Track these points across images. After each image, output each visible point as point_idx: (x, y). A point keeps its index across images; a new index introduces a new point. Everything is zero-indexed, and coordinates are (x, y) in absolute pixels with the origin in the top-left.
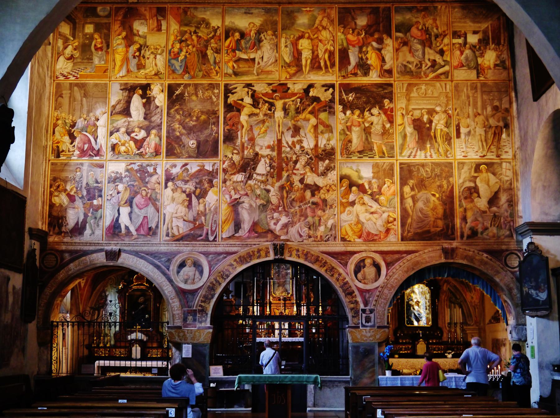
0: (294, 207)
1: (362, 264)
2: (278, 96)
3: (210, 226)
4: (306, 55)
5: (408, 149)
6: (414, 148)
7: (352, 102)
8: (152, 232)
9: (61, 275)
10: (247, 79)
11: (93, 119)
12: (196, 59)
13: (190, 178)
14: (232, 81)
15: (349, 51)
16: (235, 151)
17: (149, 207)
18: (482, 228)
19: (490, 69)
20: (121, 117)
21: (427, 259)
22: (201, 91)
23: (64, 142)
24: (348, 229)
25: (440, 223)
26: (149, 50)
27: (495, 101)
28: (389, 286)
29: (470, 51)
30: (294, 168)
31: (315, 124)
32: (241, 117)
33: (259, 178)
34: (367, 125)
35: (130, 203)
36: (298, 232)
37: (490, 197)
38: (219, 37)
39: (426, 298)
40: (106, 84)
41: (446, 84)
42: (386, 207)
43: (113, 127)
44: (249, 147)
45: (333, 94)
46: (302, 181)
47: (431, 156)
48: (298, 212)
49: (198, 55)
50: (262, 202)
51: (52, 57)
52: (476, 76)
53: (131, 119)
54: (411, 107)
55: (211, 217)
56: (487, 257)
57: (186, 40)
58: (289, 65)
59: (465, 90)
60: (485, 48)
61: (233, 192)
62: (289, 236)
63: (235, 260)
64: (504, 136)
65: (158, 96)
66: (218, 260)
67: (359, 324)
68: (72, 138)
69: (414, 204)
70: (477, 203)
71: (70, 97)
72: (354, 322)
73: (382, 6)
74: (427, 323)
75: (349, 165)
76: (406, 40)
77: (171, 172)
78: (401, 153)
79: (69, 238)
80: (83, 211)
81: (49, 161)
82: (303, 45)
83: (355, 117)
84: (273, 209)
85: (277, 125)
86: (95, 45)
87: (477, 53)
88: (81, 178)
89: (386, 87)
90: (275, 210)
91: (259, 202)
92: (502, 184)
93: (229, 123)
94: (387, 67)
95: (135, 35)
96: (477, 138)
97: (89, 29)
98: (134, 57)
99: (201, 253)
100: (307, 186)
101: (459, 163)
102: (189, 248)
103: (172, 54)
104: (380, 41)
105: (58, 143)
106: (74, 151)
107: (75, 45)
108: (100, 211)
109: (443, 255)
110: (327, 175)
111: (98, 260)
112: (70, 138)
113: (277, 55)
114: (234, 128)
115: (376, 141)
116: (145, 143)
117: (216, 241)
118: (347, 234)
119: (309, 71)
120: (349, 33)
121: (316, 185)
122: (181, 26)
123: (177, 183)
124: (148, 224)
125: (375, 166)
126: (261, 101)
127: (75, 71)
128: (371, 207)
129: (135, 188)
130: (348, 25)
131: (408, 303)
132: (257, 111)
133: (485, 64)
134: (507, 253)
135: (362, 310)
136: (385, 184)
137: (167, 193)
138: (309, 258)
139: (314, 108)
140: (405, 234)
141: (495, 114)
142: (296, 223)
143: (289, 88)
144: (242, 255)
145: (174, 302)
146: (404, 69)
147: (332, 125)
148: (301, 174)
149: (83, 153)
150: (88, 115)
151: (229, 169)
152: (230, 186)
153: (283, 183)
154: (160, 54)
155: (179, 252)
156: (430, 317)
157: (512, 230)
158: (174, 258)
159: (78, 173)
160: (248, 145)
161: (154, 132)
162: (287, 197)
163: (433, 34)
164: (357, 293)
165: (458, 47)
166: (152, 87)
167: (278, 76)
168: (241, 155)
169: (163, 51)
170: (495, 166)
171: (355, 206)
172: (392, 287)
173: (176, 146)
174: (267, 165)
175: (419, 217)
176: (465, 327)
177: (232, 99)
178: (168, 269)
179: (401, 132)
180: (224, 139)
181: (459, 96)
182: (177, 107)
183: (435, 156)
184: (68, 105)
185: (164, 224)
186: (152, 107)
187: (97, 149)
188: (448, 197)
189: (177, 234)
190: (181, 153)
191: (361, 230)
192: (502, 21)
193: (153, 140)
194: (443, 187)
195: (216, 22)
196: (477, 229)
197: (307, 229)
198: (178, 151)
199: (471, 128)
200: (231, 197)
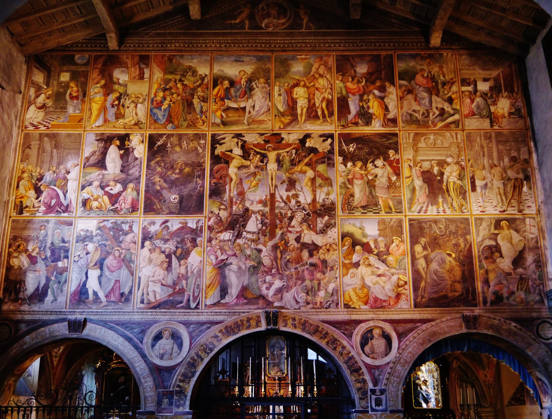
0: (290, 269)
1: (369, 335)
3: (192, 290)
4: (302, 104)
6: (424, 203)
7: (353, 152)
8: (125, 298)
9: (15, 350)
10: (236, 129)
11: (63, 171)
12: (181, 108)
13: (170, 236)
14: (220, 131)
15: (349, 99)
16: (223, 207)
17: (122, 269)
18: (508, 293)
19: (505, 117)
20: (95, 170)
21: (446, 330)
22: (185, 142)
23: (28, 197)
24: (352, 294)
25: (459, 287)
26: (129, 99)
27: (512, 152)
28: (402, 361)
29: (481, 99)
30: (289, 225)
31: (312, 177)
33: (250, 236)
34: (370, 178)
35: (100, 264)
36: (294, 297)
37: (515, 257)
38: (207, 85)
39: (433, 377)
40: (80, 134)
41: (456, 134)
42: (395, 268)
43: (86, 180)
44: (238, 202)
45: (332, 144)
46: (298, 239)
47: (444, 211)
48: (294, 275)
49: (183, 104)
50: (253, 263)
51: (22, 106)
52: (489, 126)
53: (106, 172)
54: (419, 158)
55: (194, 280)
56: (515, 327)
57: (171, 88)
58: (283, 115)
59: (478, 140)
60: (498, 96)
61: (219, 252)
62: (284, 303)
63: (221, 331)
64: (525, 189)
65: (137, 147)
66: (200, 331)
67: (367, 407)
68: (38, 192)
69: (428, 265)
70: (500, 263)
71: (39, 149)
72: (362, 405)
73: (383, 53)
74: (437, 405)
75: (352, 222)
76: (411, 88)
77: (149, 230)
78: (410, 208)
79: (27, 305)
80: (46, 274)
81: (10, 217)
82: (298, 93)
83: (357, 169)
84: (266, 272)
85: (270, 178)
86: (70, 94)
87: (489, 101)
88: (46, 236)
89: (390, 137)
90: (268, 272)
91: (249, 263)
92: (526, 242)
93: (216, 175)
94: (391, 116)
95: (115, 83)
96: (494, 191)
97: (65, 77)
98: (113, 106)
99: (180, 322)
100: (304, 246)
101: (476, 219)
102: (166, 317)
103: (154, 103)
104: (382, 89)
105: (22, 197)
106: (40, 207)
107: (48, 93)
108: (65, 274)
109: (463, 324)
110: (326, 233)
111: (59, 331)
112: (36, 193)
113: (270, 104)
114: (221, 181)
115: (382, 195)
116: (121, 198)
117: (199, 309)
118: (352, 300)
119: (305, 120)
120: (348, 81)
121: (314, 244)
122: (165, 74)
123: (155, 242)
124: (120, 289)
125: (382, 222)
126: (252, 153)
127: (46, 120)
128: (378, 268)
129: (107, 248)
130: (347, 73)
131: (414, 381)
133: (498, 112)
134: (539, 321)
135: (371, 390)
136: (393, 242)
137: (143, 254)
138: (307, 328)
139: (311, 159)
140: (419, 300)
141: (513, 165)
142: (291, 287)
143: (283, 139)
144: (229, 324)
145: (146, 382)
147: (332, 178)
148: (297, 232)
149: (50, 209)
150: (58, 168)
151: (215, 226)
152: (216, 246)
153: (276, 242)
154: (141, 103)
155: (156, 322)
156: (440, 398)
157: (543, 295)
158: (148, 328)
159: (42, 232)
160: (237, 199)
161: (131, 185)
162: (281, 257)
163: (439, 81)
164: (364, 369)
165: (468, 95)
166: (131, 137)
167: (271, 125)
169: (144, 100)
170: (518, 222)
171: (360, 268)
172: (406, 362)
173: (156, 201)
175: (434, 280)
176: (479, 410)
177: (219, 150)
178: (141, 342)
179: (409, 186)
180: (210, 194)
181: (472, 146)
182: (158, 159)
183: (448, 212)
184: (36, 156)
187: (65, 204)
188: (466, 257)
189: (153, 300)
190: (161, 208)
191: (367, 295)
192: (513, 69)
193: (130, 194)
194: (460, 246)
195: (203, 70)
196: (502, 294)
197: (304, 294)
198: (158, 206)
199: (488, 180)
200: (217, 258)
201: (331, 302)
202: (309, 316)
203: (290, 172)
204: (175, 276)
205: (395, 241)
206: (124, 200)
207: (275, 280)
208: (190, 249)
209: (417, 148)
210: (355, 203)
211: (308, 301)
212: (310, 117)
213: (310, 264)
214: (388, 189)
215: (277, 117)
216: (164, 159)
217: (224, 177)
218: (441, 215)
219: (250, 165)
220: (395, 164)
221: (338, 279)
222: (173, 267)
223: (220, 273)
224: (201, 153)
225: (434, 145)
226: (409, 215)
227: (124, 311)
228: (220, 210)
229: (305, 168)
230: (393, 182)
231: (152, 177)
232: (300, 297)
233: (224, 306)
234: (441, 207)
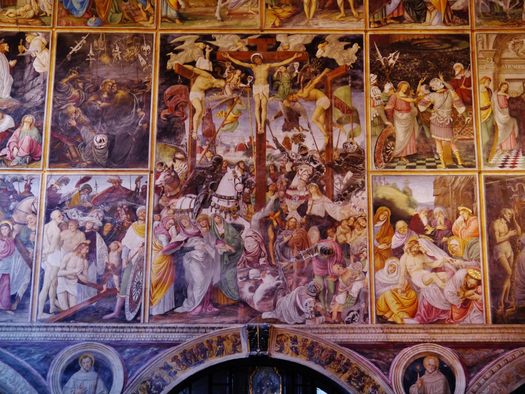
0: (289, 258)
1: (418, 367)
2: (260, 57)
3: (129, 290)
5: (500, 152)
6: (511, 151)
7: (395, 67)
13: (93, 203)
16: (179, 156)
17: (14, 256)
22: (117, 48)
24: (390, 299)
30: (288, 187)
31: (326, 107)
32: (191, 93)
33: (223, 203)
34: (422, 109)
36: (295, 304)
42: (462, 258)
44: (205, 147)
45: (359, 53)
46: (302, 210)
48: (295, 268)
50: (228, 248)
54: (503, 77)
55: (132, 276)
61: (173, 230)
62: (279, 313)
63: (175, 359)
66: (142, 359)
69: (516, 254)
75: (391, 181)
77: (59, 192)
78: (487, 160)
83: (401, 94)
84: (249, 262)
85: (257, 109)
90: (253, 263)
91: (222, 248)
93: (169, 103)
99: (109, 344)
100: (313, 220)
102: (86, 335)
110: (349, 199)
114: (177, 113)
116: (11, 139)
117: (139, 322)
118: (389, 310)
119: (316, 13)
121: (328, 217)
123: (69, 212)
124: (9, 289)
125: (439, 183)
128: (433, 258)
132: (222, 83)
136: (458, 215)
138: (316, 356)
139: (324, 78)
140: (500, 310)
142: (291, 288)
143: (279, 43)
144: (188, 348)
146: (489, 10)
147: (359, 109)
148: (301, 198)
151: (167, 187)
153: (266, 214)
155: (68, 343)
158: (56, 353)
160: (203, 143)
161: (28, 119)
162: (275, 238)
166: (28, 39)
167: (259, 22)
168: (190, 161)
171: (403, 257)
173: (69, 144)
174: (237, 181)
177: (174, 62)
178: (45, 376)
179: (486, 122)
182: (73, 75)
185: (41, 289)
186: (26, 75)
189: (64, 307)
190: (79, 157)
191: (415, 302)
197: (311, 299)
198: (74, 153)
200: (170, 239)
201: (355, 313)
202: (319, 336)
203: (291, 99)
204: (100, 269)
205: (461, 213)
206: (17, 142)
207: (264, 276)
208: (125, 225)
209: (501, 59)
210: (397, 151)
211: (319, 310)
212: (323, 8)
213: (322, 250)
214: (452, 128)
215: (270, 8)
216: (83, 75)
217: (182, 106)
219: (224, 87)
220: (463, 87)
221: (368, 275)
222: (98, 254)
223: (175, 264)
224: (144, 66)
226: (485, 171)
227: (16, 324)
228: (174, 161)
229: (314, 92)
230: (459, 116)
231: (63, 105)
232: (304, 304)
233: (181, 318)
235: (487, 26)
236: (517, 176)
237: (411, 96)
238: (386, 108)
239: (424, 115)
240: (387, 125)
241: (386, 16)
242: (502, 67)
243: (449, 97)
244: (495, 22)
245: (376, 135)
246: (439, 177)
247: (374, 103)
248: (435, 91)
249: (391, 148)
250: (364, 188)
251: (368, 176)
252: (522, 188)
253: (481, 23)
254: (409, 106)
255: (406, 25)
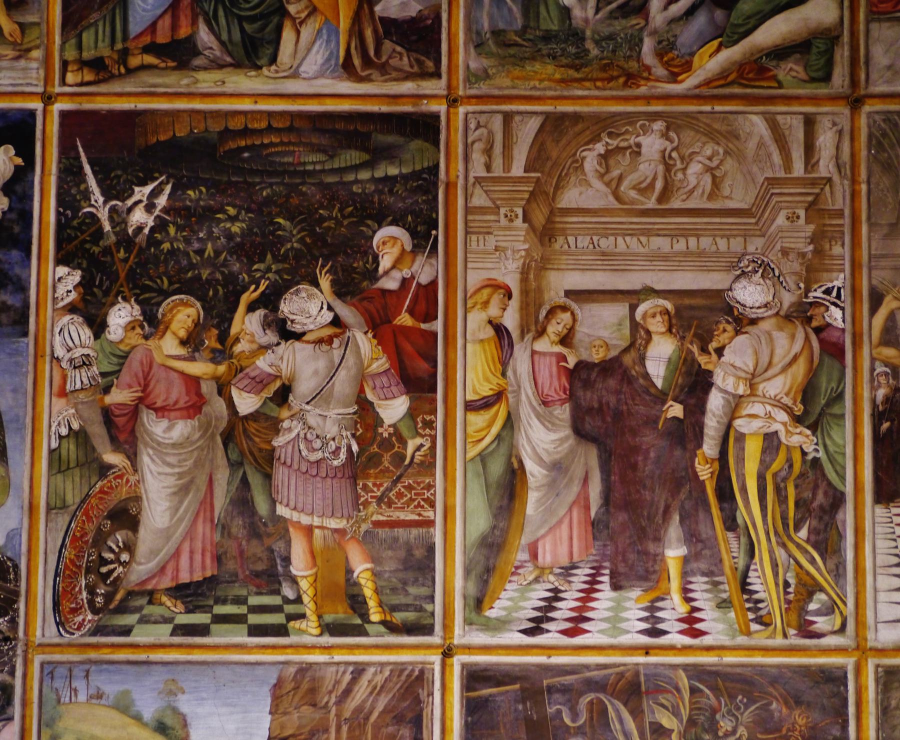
6: (568, 571)
7: (152, 241)
41: (810, 122)
75: (111, 688)
78: (478, 603)
83: (169, 345)
146: (519, 23)
179: (483, 457)
214: (354, 479)
218: (671, 648)
220: (405, 319)
225: (664, 196)
226: (469, 649)
230: (384, 432)
234: (676, 597)
235: (507, 82)
236: (587, 667)
237: (206, 354)
238: (108, 400)
239: (252, 427)
240: (111, 467)
241: (125, 38)
242: (557, 246)
243: (350, 359)
244: (538, 66)
245: (64, 507)
246: (292, 670)
247: (64, 378)
248: (298, 336)
249: (118, 555)
250: (9, 711)
251: (26, 663)
252: (604, 712)
253: (485, 71)
254: (199, 395)
255: (201, 75)
